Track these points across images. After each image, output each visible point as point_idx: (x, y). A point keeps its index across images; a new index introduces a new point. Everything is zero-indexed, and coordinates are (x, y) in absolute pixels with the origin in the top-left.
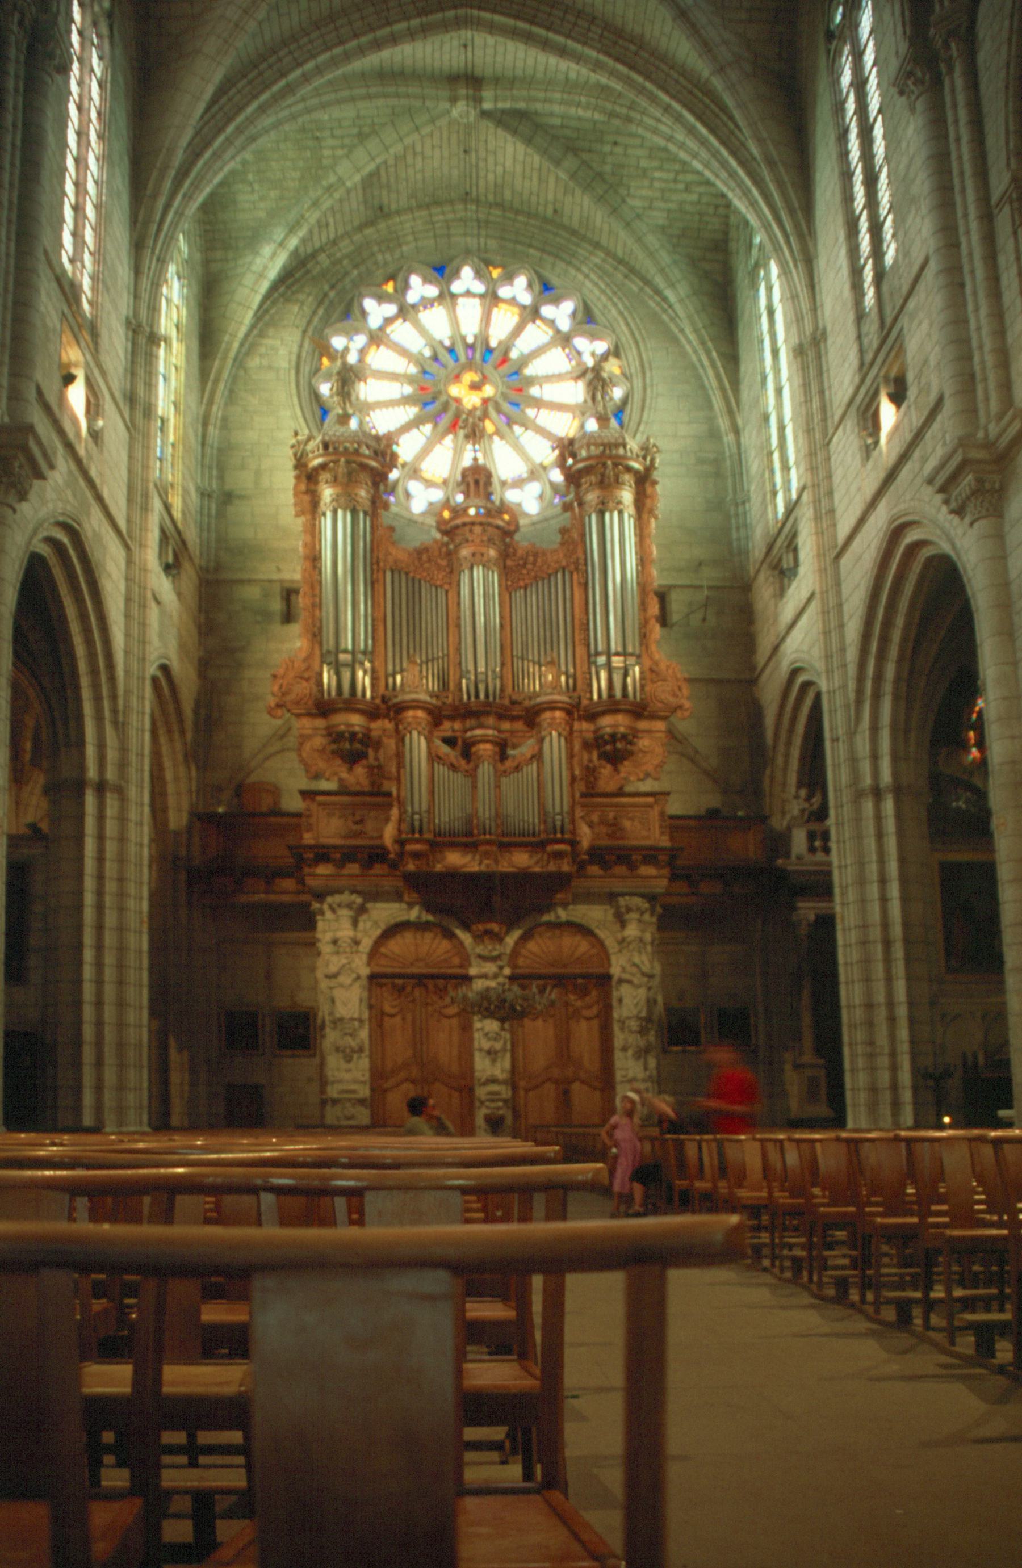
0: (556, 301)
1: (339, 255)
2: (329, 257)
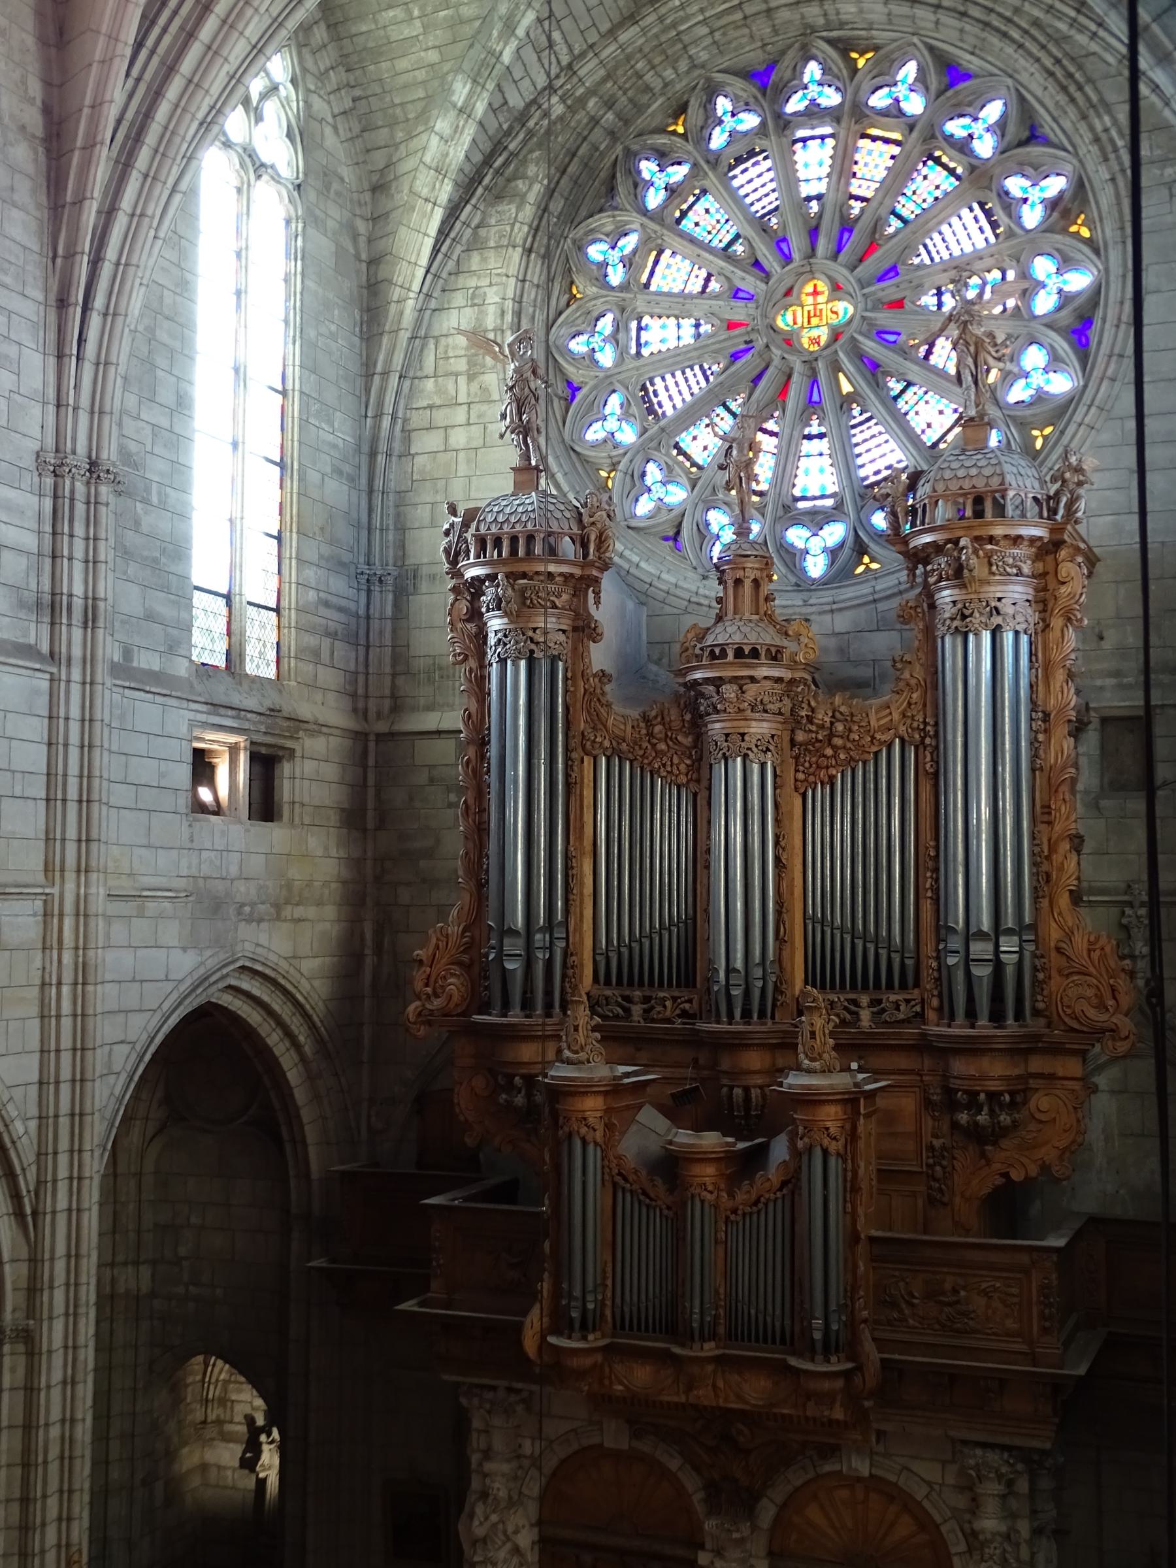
0: (968, 108)
1: (580, 91)
2: (563, 99)
